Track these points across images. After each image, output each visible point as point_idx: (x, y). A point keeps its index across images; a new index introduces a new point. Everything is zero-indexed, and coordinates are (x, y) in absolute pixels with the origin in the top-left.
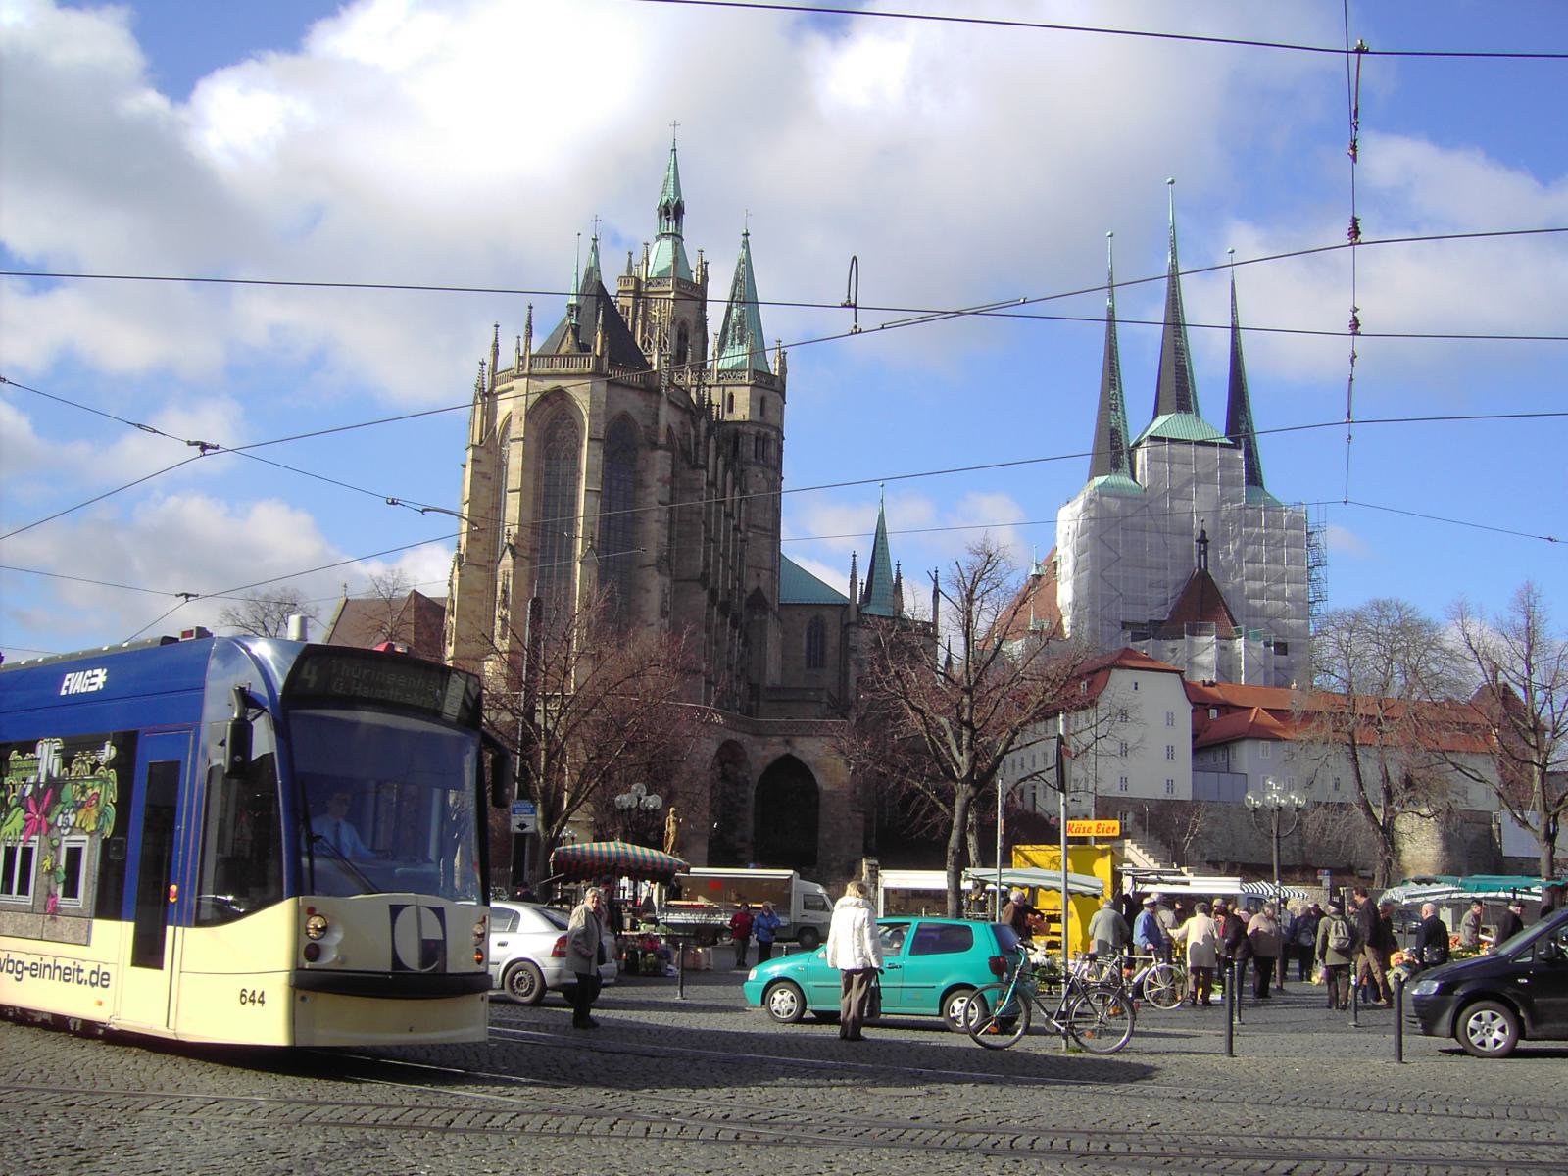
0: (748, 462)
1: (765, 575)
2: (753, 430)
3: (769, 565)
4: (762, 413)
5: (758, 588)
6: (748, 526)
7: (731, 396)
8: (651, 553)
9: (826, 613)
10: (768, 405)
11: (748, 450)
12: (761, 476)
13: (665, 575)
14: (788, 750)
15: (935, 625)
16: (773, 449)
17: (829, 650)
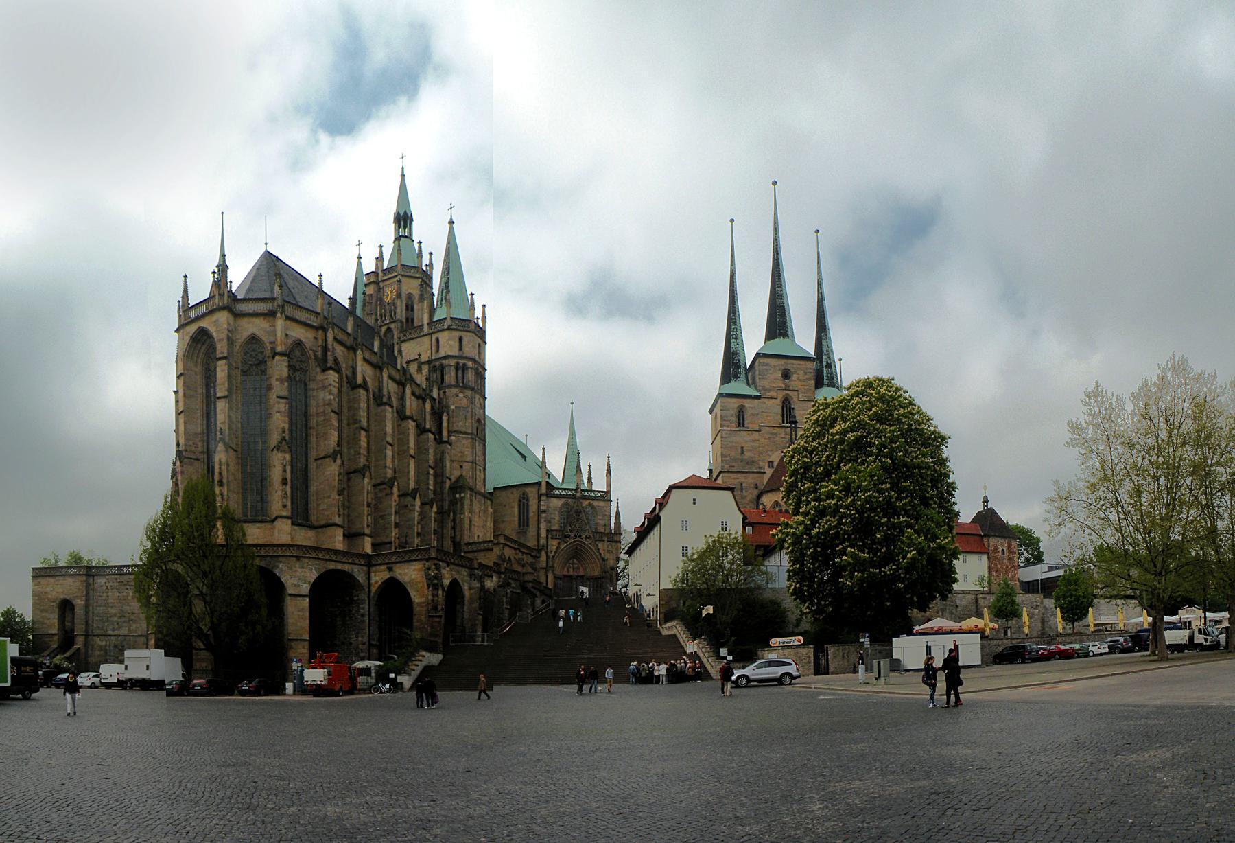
0: (450, 386)
1: (466, 466)
2: (453, 362)
3: (469, 459)
4: (461, 349)
5: (461, 476)
6: (450, 433)
7: (437, 340)
8: (275, 438)
9: (528, 490)
10: (464, 343)
11: (450, 377)
12: (461, 395)
13: (285, 452)
14: (391, 574)
15: (608, 492)
16: (470, 375)
17: (531, 514)
